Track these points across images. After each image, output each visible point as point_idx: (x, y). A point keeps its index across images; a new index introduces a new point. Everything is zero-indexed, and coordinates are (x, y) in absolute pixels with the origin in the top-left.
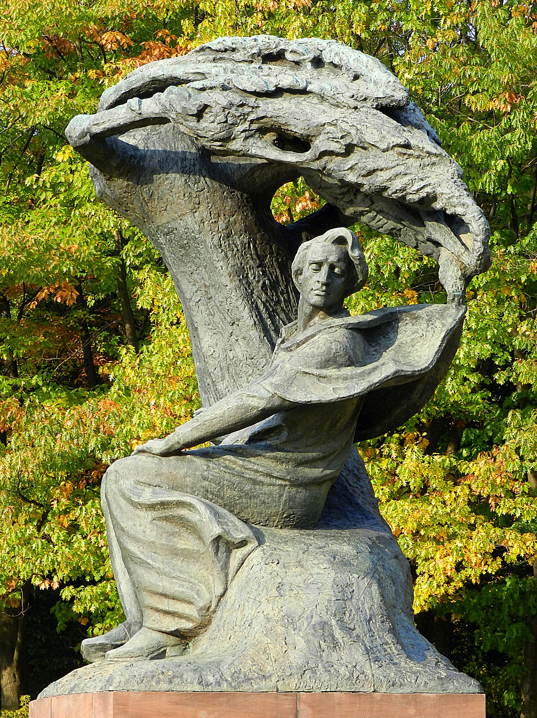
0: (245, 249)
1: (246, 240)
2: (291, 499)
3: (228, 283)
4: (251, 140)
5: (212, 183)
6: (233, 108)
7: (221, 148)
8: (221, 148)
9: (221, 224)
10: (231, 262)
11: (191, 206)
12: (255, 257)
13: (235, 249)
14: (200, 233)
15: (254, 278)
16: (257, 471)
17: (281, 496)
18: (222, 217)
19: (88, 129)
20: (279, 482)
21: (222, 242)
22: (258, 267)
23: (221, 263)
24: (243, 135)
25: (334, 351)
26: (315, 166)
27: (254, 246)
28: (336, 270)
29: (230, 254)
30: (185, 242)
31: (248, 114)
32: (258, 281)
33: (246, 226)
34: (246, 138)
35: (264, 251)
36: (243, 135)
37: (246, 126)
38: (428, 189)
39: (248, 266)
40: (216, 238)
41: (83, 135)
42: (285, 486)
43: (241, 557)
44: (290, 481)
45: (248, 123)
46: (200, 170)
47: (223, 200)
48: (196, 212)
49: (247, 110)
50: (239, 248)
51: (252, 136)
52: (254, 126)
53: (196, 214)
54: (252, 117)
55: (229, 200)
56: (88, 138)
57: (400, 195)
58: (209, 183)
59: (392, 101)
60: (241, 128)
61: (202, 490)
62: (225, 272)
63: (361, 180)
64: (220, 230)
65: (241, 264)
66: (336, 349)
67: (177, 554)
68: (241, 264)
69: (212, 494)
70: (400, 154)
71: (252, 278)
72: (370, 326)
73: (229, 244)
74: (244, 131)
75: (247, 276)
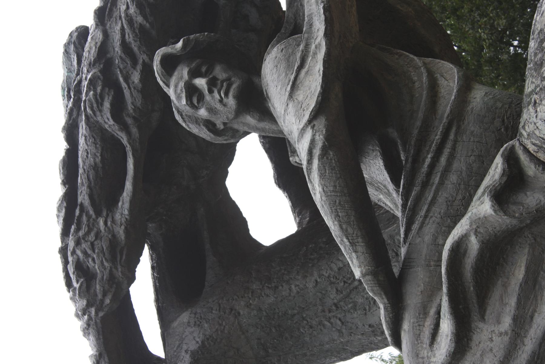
3: (313, 279)
7: (125, 253)
8: (125, 253)
14: (260, 309)
16: (432, 166)
20: (452, 136)
23: (293, 287)
24: (109, 223)
26: (134, 130)
30: (274, 330)
31: (89, 217)
34: (113, 221)
40: (268, 291)
42: (459, 127)
43: (533, 166)
48: (239, 313)
54: (91, 212)
57: (148, 10)
63: (139, 67)
67: (535, 282)
70: (110, 16)
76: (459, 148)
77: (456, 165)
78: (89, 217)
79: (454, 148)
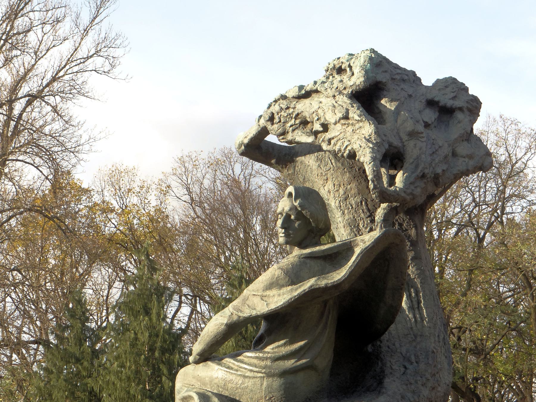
0: (358, 206)
1: (359, 200)
2: (268, 386)
4: (296, 131)
5: (336, 164)
6: (283, 112)
9: (341, 191)
10: (347, 217)
11: (321, 183)
12: (365, 211)
13: (350, 208)
15: (363, 226)
17: (262, 385)
18: (342, 187)
19: (242, 141)
21: (342, 204)
22: (367, 218)
24: (291, 128)
25: (276, 276)
27: (366, 203)
28: (293, 217)
29: (346, 211)
31: (292, 113)
32: (366, 228)
33: (359, 190)
34: (293, 130)
35: (374, 206)
36: (291, 128)
37: (293, 121)
38: (349, 148)
39: (359, 218)
40: (338, 202)
41: (240, 146)
42: (264, 377)
44: (265, 373)
45: (293, 120)
46: (329, 156)
47: (343, 174)
49: (291, 110)
50: (354, 206)
51: (297, 128)
52: (298, 122)
53: (326, 188)
55: (348, 173)
56: (243, 147)
58: (334, 164)
59: (356, 86)
60: (289, 125)
61: (215, 386)
62: (341, 225)
64: (340, 196)
65: (354, 217)
66: (278, 275)
68: (354, 217)
69: (221, 388)
70: (343, 125)
71: (361, 226)
72: (326, 253)
73: (346, 205)
74: (291, 126)
75: (358, 225)
76: (255, 380)
77: (247, 380)
78: (292, 113)
79: (254, 377)
